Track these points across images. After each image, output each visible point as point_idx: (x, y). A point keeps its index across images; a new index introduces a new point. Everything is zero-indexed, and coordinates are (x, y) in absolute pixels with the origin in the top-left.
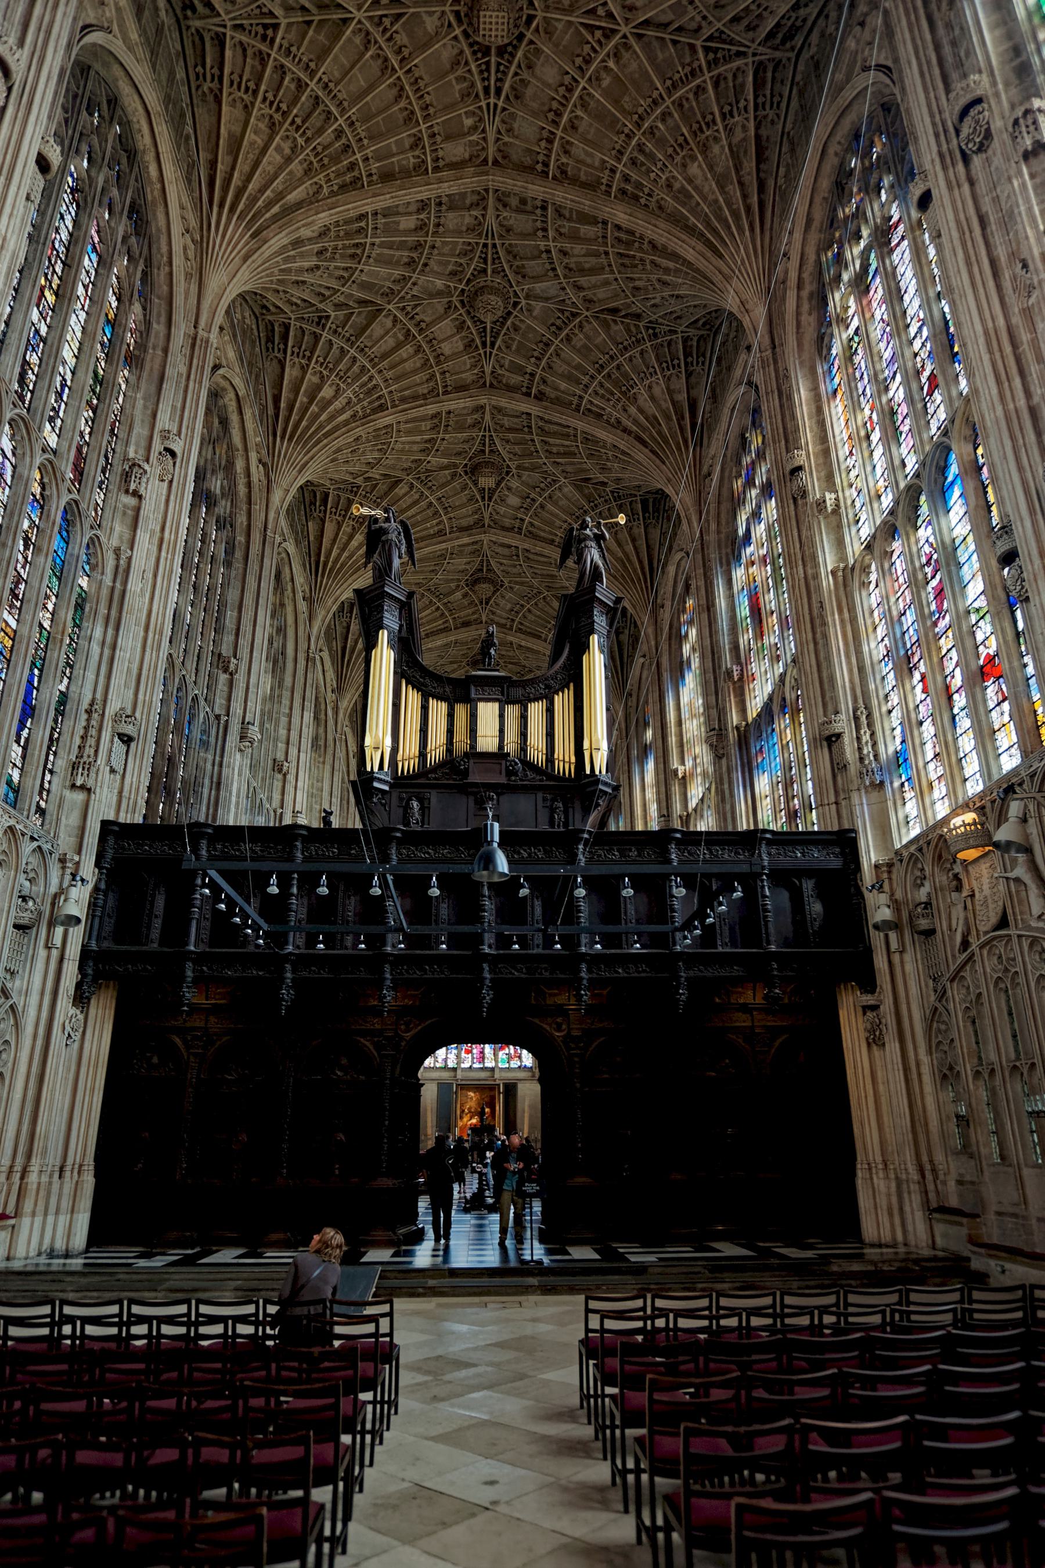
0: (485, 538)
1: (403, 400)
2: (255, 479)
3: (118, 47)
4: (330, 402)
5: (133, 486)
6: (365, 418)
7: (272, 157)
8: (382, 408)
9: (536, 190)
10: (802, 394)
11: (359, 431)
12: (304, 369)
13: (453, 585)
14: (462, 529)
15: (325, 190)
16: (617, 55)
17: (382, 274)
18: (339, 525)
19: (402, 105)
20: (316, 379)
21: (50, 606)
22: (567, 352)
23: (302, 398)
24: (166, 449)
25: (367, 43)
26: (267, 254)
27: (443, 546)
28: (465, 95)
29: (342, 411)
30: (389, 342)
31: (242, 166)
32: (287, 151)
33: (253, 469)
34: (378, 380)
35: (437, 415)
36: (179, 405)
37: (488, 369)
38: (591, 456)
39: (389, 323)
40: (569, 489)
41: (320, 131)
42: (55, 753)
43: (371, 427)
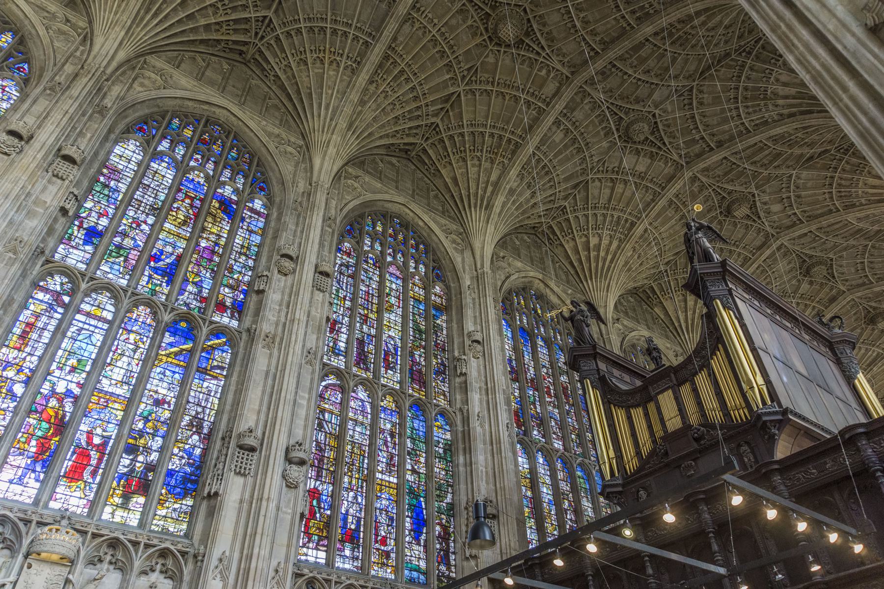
3: (369, 197)
5: (459, 372)
7: (473, 171)
8: (633, 224)
13: (794, 282)
14: (760, 248)
15: (506, 162)
19: (507, 98)
20: (584, 239)
21: (422, 460)
22: (708, 110)
23: (583, 254)
24: (474, 341)
25: (474, 93)
26: (498, 211)
28: (531, 66)
30: (607, 191)
32: (477, 163)
34: (616, 214)
35: (671, 202)
36: (478, 314)
38: (791, 146)
39: (597, 183)
42: (454, 541)
43: (634, 239)
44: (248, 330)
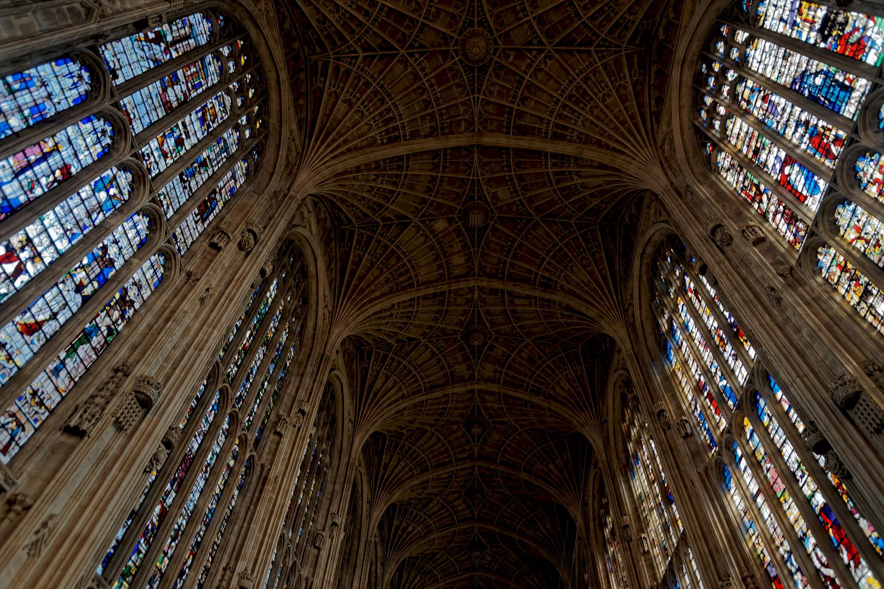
0: (476, 574)
1: (441, 527)
2: (379, 574)
4: (410, 533)
6: (425, 536)
7: (399, 467)
8: (432, 531)
9: (493, 467)
10: (600, 567)
11: (422, 542)
12: (401, 522)
16: (519, 435)
17: (436, 491)
18: (410, 574)
22: (508, 510)
23: (400, 532)
27: (456, 579)
29: (416, 535)
30: (436, 508)
31: (388, 472)
33: (379, 570)
34: (431, 522)
37: (476, 513)
39: (436, 502)
40: (513, 555)
41: (416, 458)
44: (307, 579)
